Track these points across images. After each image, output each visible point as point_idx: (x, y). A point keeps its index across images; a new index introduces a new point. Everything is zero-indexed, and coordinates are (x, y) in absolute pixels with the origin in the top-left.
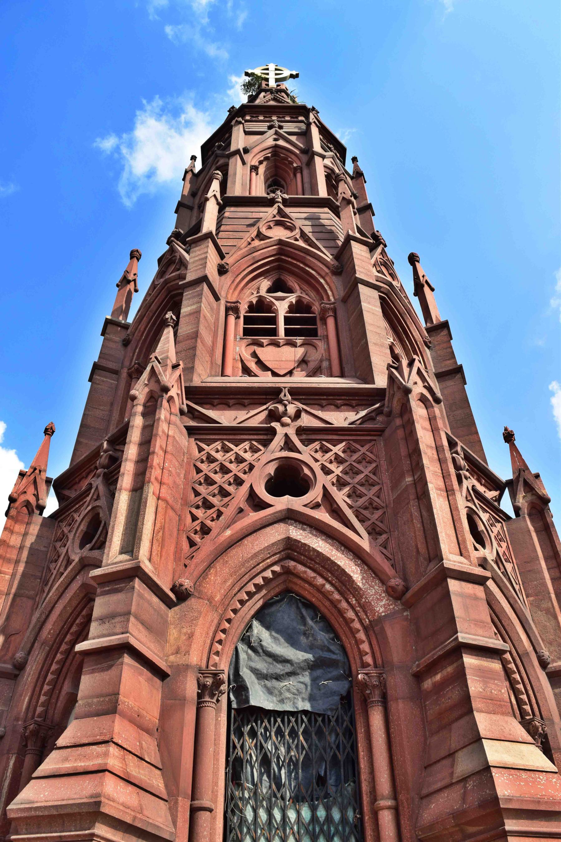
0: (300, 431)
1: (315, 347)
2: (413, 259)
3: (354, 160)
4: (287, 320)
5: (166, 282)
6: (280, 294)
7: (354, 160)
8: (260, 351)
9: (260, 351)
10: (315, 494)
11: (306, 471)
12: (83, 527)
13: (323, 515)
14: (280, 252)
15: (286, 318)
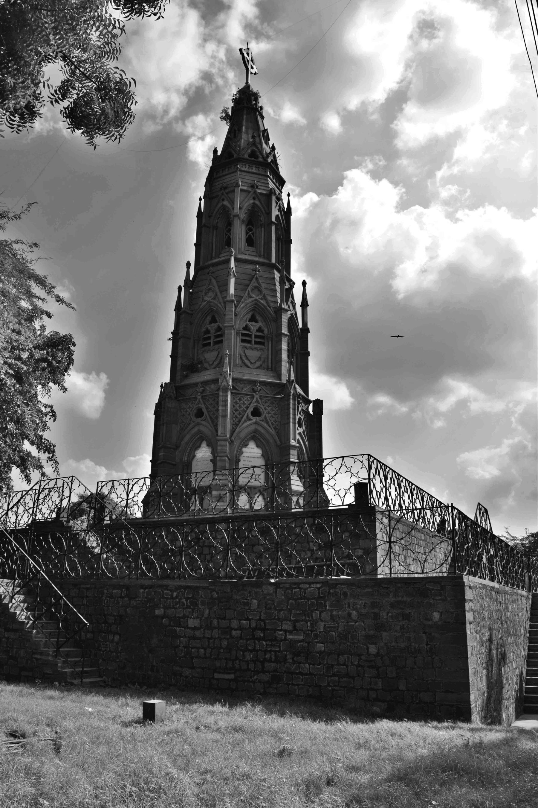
0: (260, 396)
1: (263, 351)
2: (304, 283)
3: (289, 195)
4: (256, 336)
5: (209, 302)
6: (254, 323)
7: (289, 195)
8: (246, 351)
9: (246, 351)
10: (263, 417)
11: (261, 410)
12: (195, 411)
13: (265, 424)
14: (256, 304)
15: (255, 335)
